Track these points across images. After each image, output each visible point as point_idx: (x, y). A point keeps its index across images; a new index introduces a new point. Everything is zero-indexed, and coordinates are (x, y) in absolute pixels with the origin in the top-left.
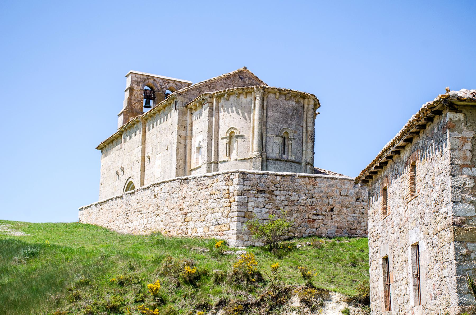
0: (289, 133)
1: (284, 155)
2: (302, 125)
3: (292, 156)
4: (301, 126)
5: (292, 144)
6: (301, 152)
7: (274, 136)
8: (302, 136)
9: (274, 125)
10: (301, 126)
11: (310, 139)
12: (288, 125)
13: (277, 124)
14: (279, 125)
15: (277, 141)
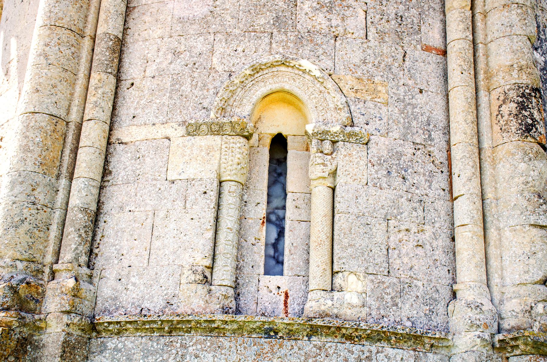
0: (304, 97)
1: (274, 280)
2: (435, 40)
3: (338, 280)
4: (427, 49)
5: (341, 180)
6: (443, 241)
7: (169, 131)
8: (439, 115)
9: (176, 54)
10: (427, 49)
11: (514, 125)
12: (300, 39)
13: (200, 45)
14: (219, 48)
15: (190, 173)
